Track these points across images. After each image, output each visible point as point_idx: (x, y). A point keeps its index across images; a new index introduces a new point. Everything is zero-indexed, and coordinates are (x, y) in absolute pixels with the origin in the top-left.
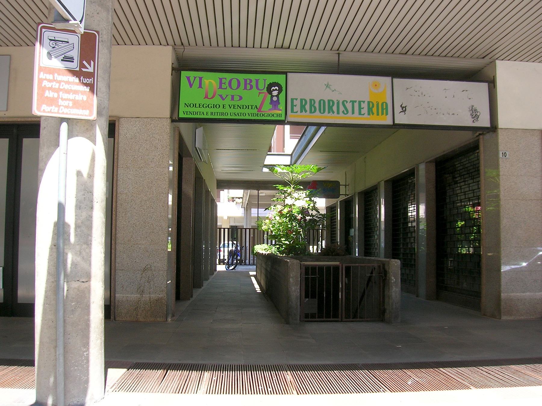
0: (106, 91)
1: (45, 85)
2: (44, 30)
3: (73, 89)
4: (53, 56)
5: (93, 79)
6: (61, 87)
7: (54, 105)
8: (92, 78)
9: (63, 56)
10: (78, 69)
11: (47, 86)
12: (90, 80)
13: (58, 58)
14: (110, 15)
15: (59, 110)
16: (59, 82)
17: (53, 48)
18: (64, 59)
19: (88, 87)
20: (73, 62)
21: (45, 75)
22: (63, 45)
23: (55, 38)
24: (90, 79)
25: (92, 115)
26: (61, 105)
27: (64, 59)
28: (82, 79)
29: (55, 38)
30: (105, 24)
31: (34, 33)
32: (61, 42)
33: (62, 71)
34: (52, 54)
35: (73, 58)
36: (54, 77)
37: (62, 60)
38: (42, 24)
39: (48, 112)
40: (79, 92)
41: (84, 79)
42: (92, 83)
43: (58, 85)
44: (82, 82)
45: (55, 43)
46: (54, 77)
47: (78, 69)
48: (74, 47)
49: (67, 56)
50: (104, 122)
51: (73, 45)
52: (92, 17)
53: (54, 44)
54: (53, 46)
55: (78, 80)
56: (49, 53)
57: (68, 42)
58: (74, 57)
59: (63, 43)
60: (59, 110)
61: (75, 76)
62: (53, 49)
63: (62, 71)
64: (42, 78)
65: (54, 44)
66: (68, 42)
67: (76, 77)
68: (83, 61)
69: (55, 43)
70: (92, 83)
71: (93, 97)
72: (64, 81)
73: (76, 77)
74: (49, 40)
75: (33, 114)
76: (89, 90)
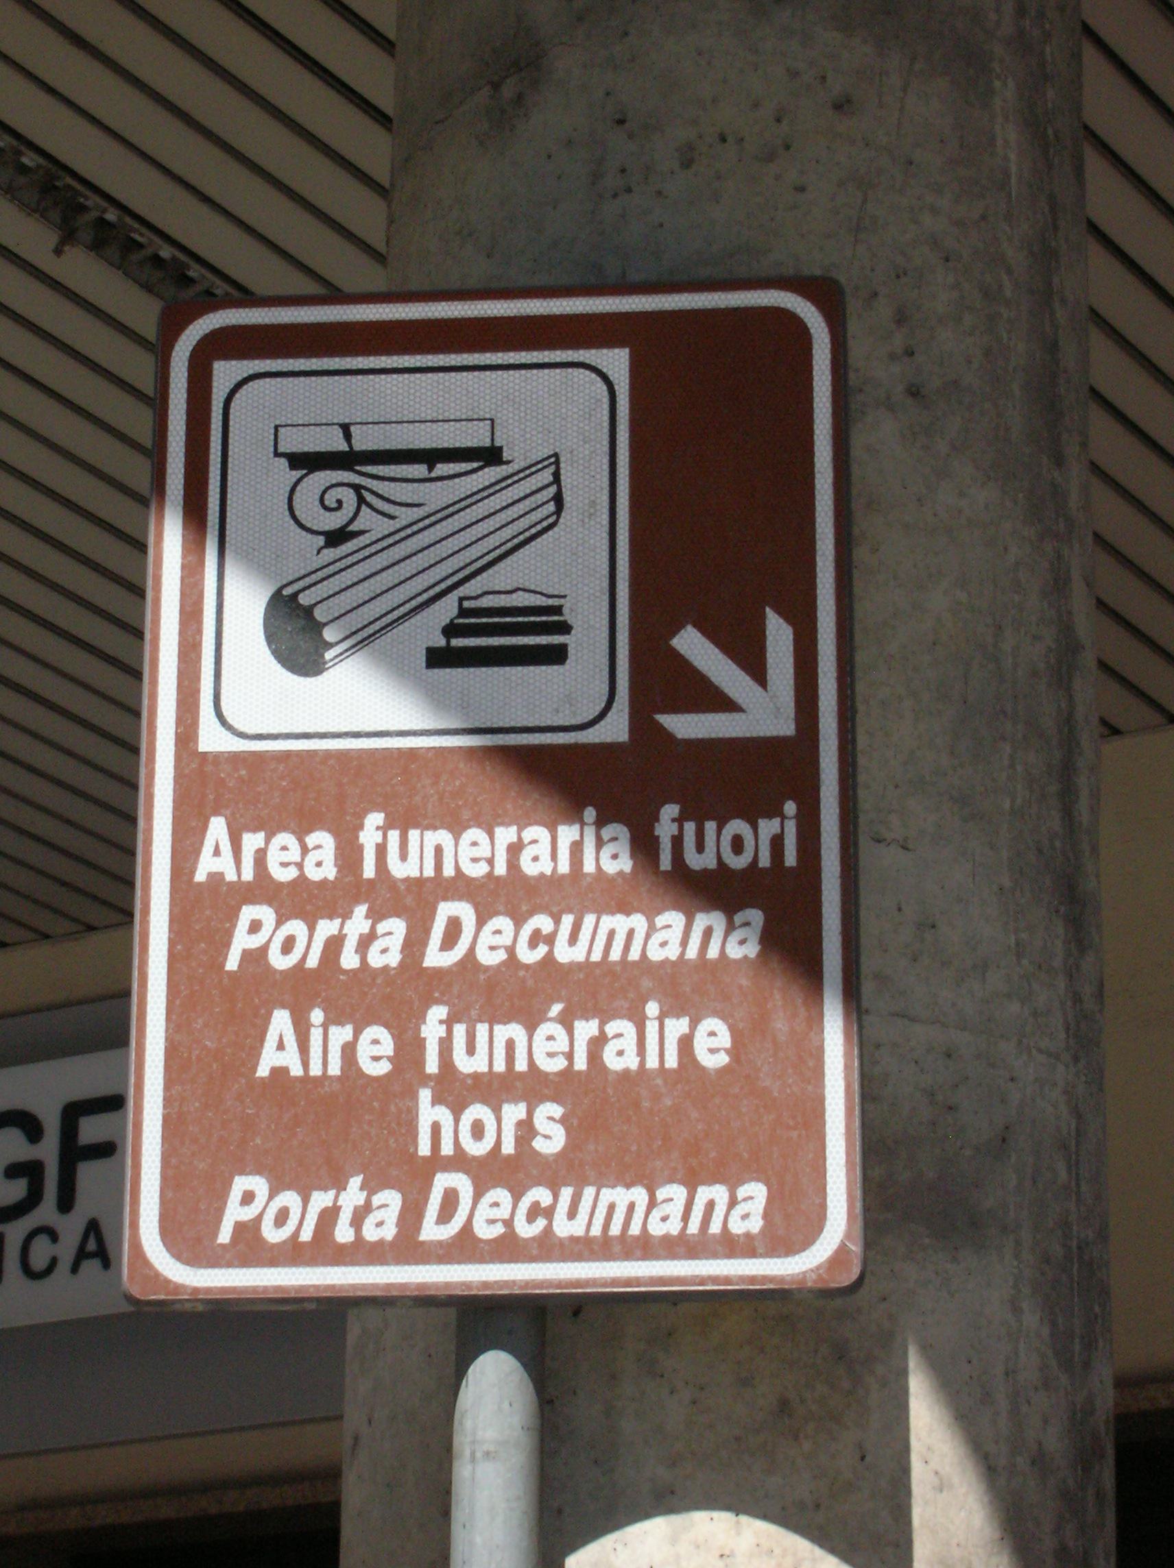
0: (1020, 951)
1: (256, 957)
2: (225, 373)
3: (565, 954)
4: (329, 634)
5: (798, 816)
6: (435, 958)
7: (363, 1169)
8: (790, 808)
9: (446, 610)
10: (616, 729)
11: (280, 962)
12: (768, 827)
13: (379, 643)
14: (997, 102)
15: (411, 1216)
16: (409, 901)
17: (336, 538)
18: (457, 642)
19: (738, 918)
20: (557, 655)
21: (252, 841)
22: (437, 495)
23: (348, 436)
24: (762, 823)
25: (807, 1242)
26: (436, 1163)
27: (457, 642)
28: (665, 829)
29: (348, 436)
30: (934, 211)
31: (139, 423)
32: (419, 470)
33: (437, 777)
34: (320, 614)
35: (558, 610)
36: (349, 855)
37: (437, 658)
38: (212, 303)
39: (293, 1253)
40: (646, 983)
41: (690, 828)
42: (790, 859)
43: (395, 929)
44: (666, 862)
45: (357, 488)
46: (349, 855)
47: (616, 729)
48: (558, 499)
49: (486, 602)
50: (1016, 1310)
51: (546, 476)
52: (770, 157)
53: (340, 502)
54: (333, 521)
55: (623, 847)
56: (295, 596)
57: (491, 455)
58: (567, 604)
59: (442, 469)
60: (411, 1216)
61: (590, 814)
62: (330, 554)
63: (437, 777)
64: (678, 1017)
65: (340, 502)
66: (491, 455)
67: (600, 823)
68: (675, 629)
69: (357, 488)
70: (790, 859)
71: (817, 1021)
72: (460, 887)
73: (600, 823)
74: (284, 462)
75: (130, 1299)
76: (752, 950)
